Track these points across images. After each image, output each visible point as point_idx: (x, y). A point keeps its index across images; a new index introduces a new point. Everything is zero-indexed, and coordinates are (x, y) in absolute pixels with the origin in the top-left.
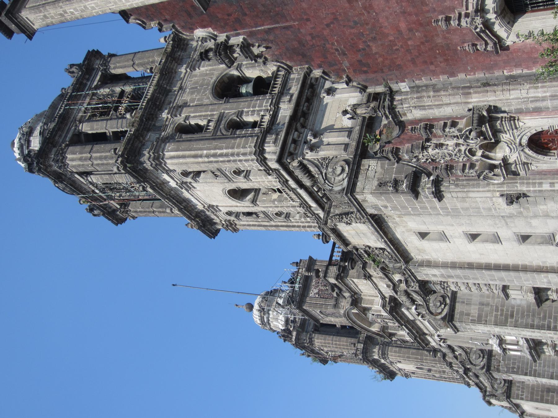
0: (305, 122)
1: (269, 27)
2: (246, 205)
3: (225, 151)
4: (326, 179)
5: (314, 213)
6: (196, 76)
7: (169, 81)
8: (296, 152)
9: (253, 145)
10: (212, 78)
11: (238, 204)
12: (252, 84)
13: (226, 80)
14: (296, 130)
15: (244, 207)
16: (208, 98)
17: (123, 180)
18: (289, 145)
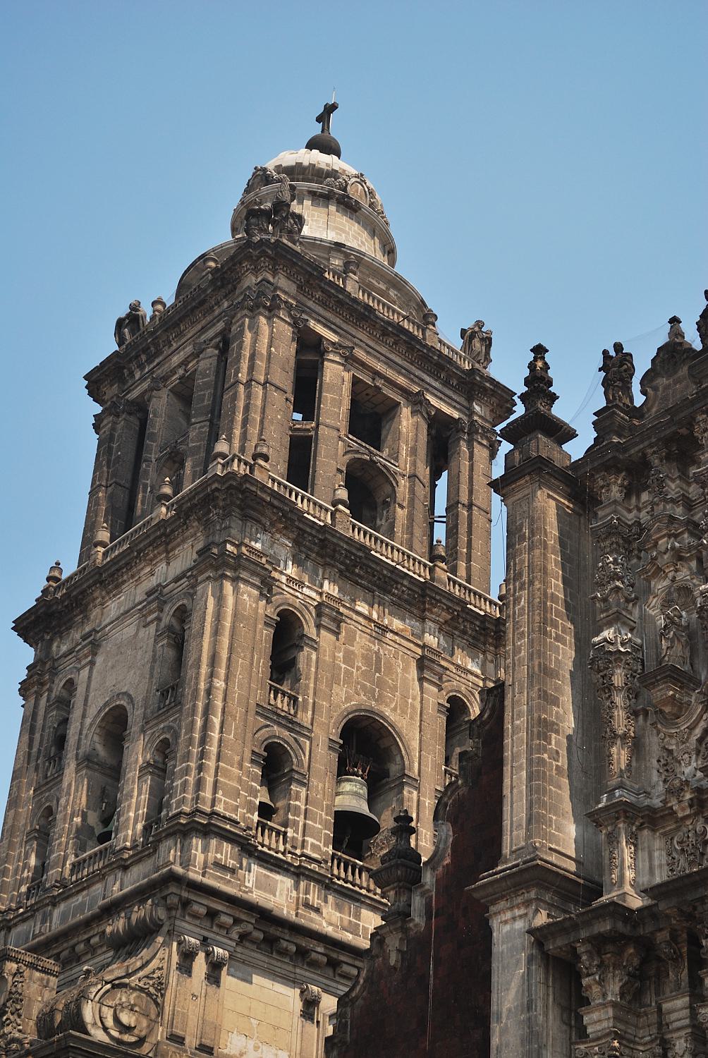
0: (253, 942)
1: (431, 987)
2: (83, 742)
3: (215, 735)
4: (114, 987)
5: (38, 910)
6: (405, 670)
7: (406, 601)
8: (187, 918)
9: (220, 808)
10: (394, 709)
11: (88, 721)
12: (364, 808)
13: (384, 743)
14: (237, 921)
15: (81, 734)
16: (348, 699)
17: (193, 441)
18: (205, 902)
